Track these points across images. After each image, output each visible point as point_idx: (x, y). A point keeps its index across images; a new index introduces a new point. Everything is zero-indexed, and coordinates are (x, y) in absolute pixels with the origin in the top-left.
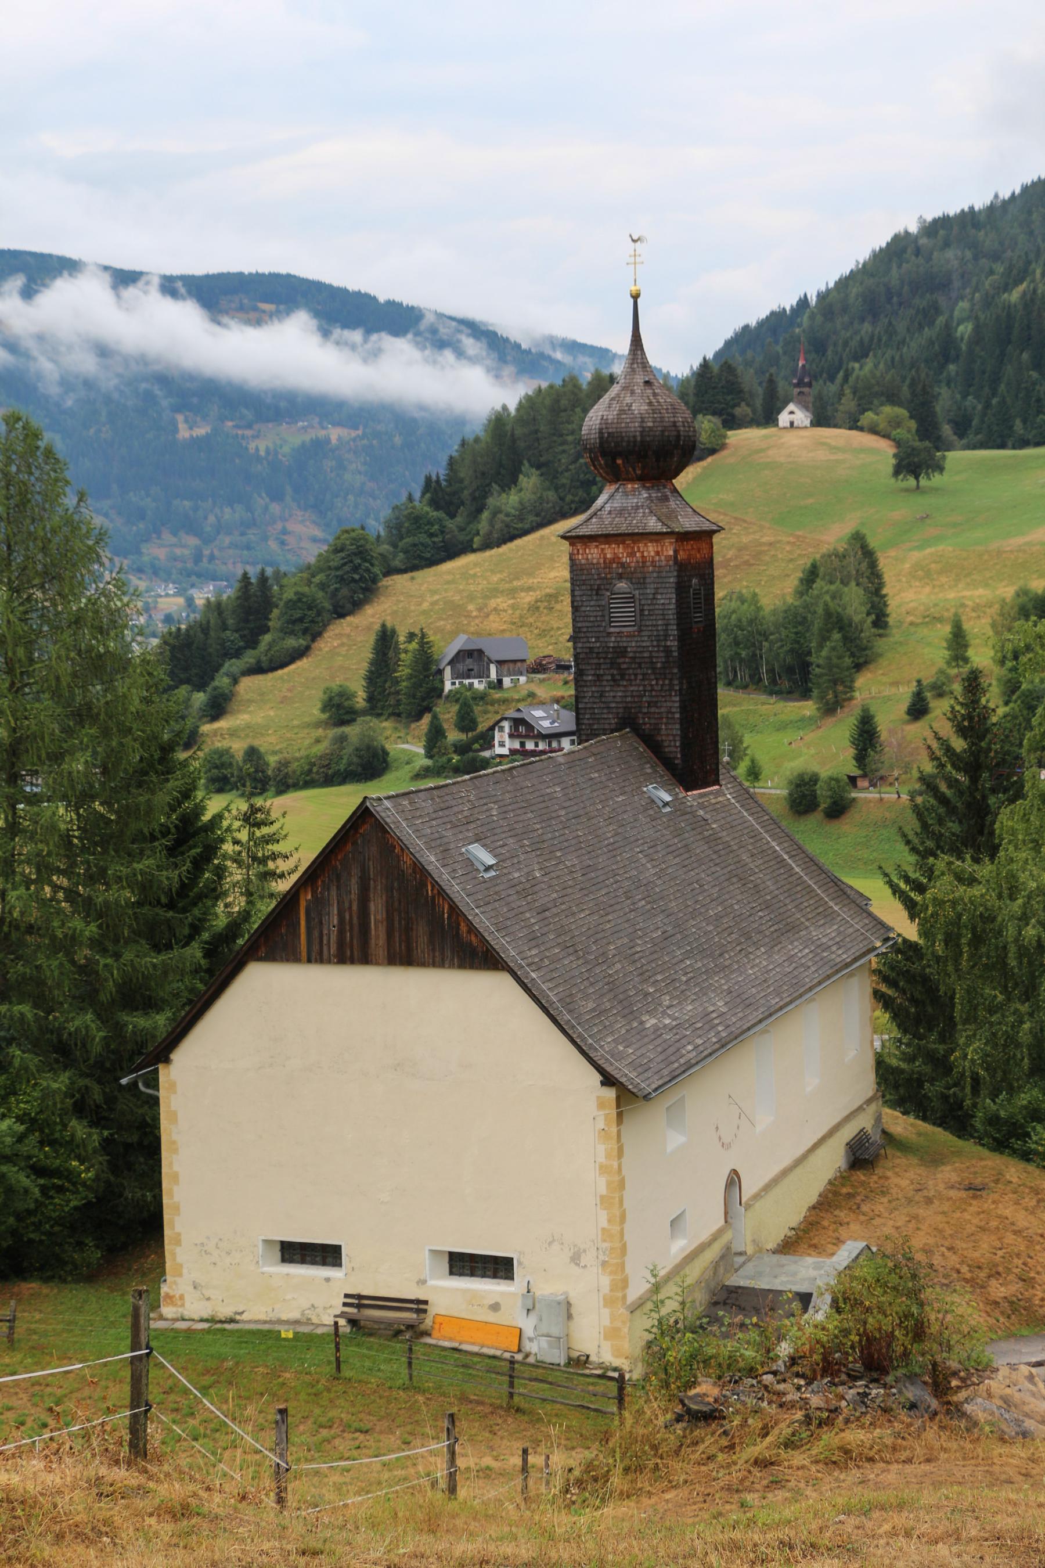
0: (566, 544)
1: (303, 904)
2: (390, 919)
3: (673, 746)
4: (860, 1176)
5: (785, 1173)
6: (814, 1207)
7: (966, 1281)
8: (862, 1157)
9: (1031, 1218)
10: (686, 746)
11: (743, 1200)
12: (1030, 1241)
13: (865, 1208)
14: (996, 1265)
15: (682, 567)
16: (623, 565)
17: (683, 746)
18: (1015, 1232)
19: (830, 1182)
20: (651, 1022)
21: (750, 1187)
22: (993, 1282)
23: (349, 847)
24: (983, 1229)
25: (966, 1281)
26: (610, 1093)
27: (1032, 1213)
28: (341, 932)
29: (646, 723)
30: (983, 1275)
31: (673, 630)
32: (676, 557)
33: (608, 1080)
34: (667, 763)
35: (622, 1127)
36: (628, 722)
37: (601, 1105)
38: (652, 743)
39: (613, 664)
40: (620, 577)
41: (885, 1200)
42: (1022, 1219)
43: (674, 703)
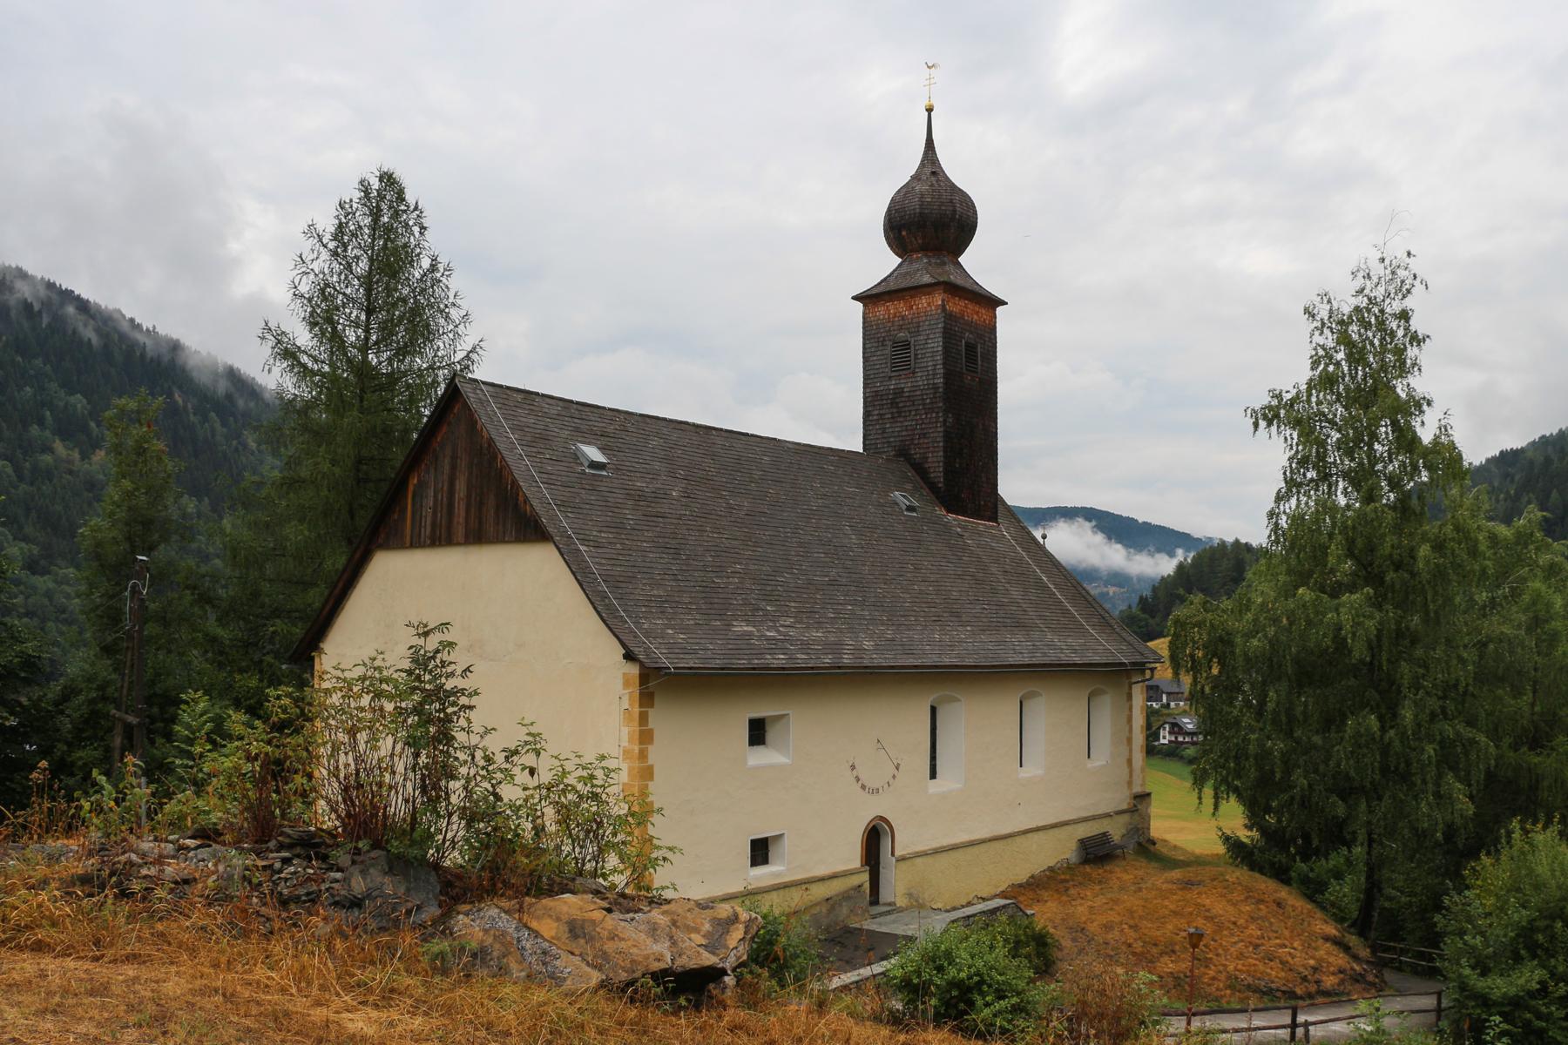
0: (859, 306)
1: (411, 488)
2: (469, 496)
3: (937, 470)
4: (1088, 868)
5: (972, 844)
6: (1020, 886)
7: (1134, 954)
8: (1096, 853)
9: (1230, 909)
10: (949, 471)
11: (898, 853)
12: (1220, 927)
13: (1072, 892)
14: (1173, 943)
15: (949, 318)
16: (903, 318)
17: (946, 472)
18: (1206, 918)
19: (1051, 869)
20: (741, 627)
21: (907, 839)
22: (1166, 959)
23: (445, 429)
24: (1175, 913)
25: (1134, 954)
26: (634, 670)
27: (1235, 905)
28: (435, 513)
29: (916, 453)
30: (1155, 950)
31: (940, 370)
32: (943, 306)
33: (629, 656)
34: (932, 487)
35: (651, 712)
36: (903, 453)
37: (626, 684)
38: (920, 470)
39: (894, 404)
40: (901, 328)
41: (1098, 887)
42: (1219, 908)
43: (937, 434)
